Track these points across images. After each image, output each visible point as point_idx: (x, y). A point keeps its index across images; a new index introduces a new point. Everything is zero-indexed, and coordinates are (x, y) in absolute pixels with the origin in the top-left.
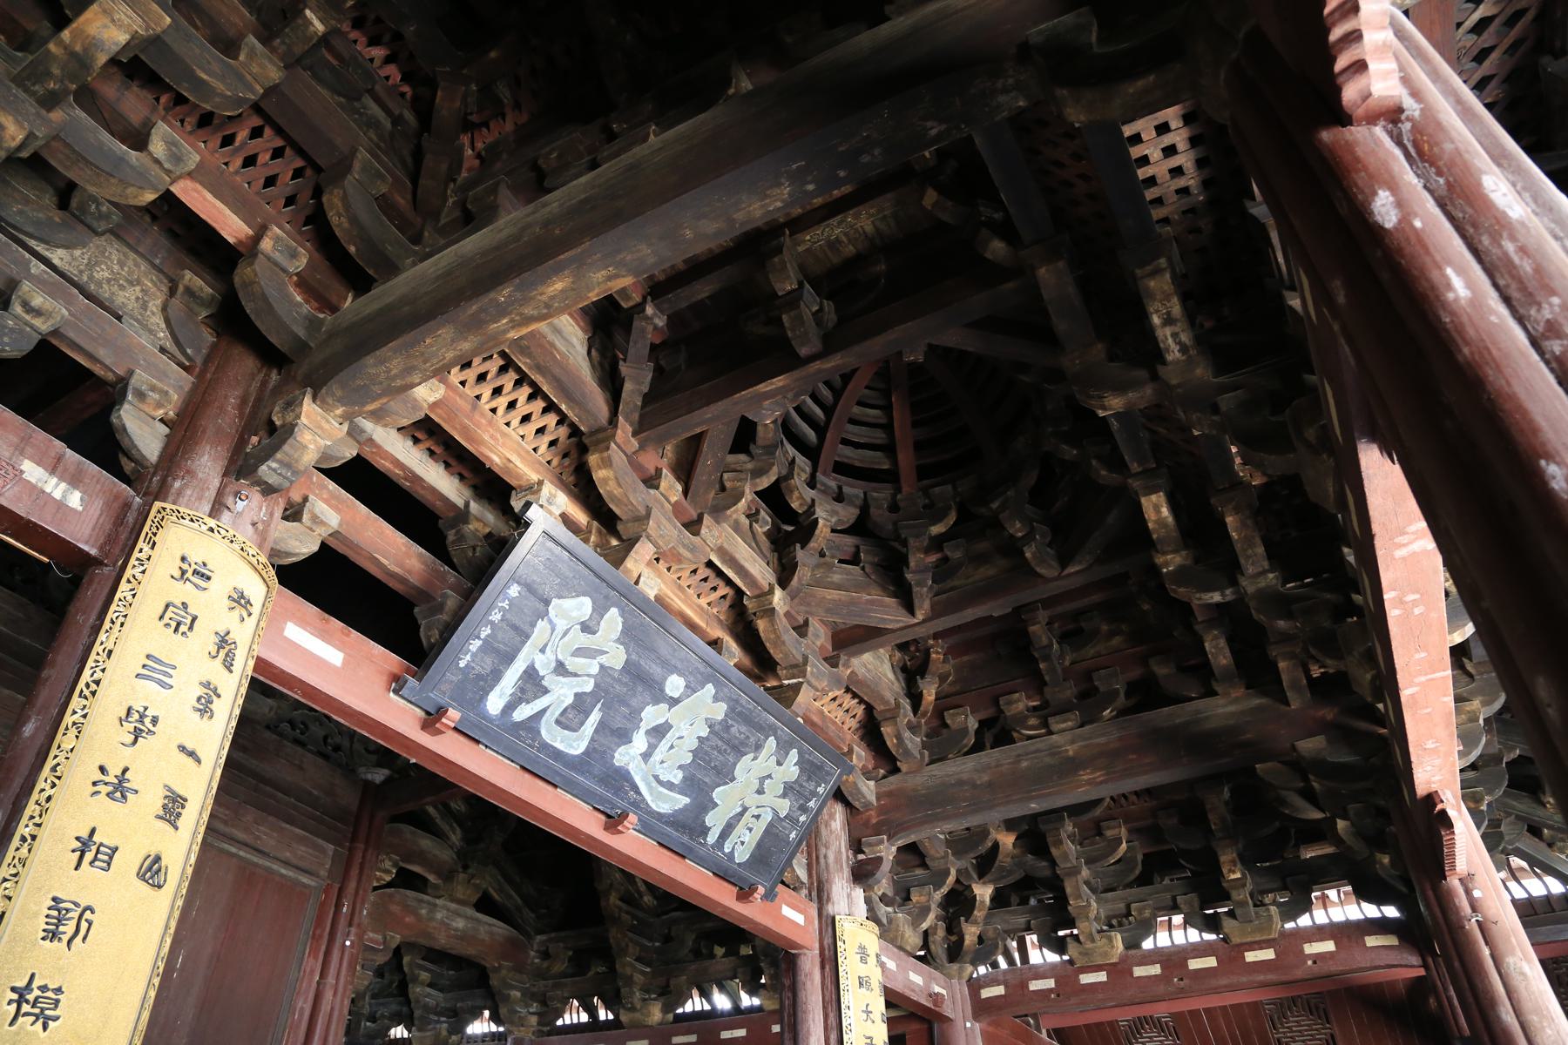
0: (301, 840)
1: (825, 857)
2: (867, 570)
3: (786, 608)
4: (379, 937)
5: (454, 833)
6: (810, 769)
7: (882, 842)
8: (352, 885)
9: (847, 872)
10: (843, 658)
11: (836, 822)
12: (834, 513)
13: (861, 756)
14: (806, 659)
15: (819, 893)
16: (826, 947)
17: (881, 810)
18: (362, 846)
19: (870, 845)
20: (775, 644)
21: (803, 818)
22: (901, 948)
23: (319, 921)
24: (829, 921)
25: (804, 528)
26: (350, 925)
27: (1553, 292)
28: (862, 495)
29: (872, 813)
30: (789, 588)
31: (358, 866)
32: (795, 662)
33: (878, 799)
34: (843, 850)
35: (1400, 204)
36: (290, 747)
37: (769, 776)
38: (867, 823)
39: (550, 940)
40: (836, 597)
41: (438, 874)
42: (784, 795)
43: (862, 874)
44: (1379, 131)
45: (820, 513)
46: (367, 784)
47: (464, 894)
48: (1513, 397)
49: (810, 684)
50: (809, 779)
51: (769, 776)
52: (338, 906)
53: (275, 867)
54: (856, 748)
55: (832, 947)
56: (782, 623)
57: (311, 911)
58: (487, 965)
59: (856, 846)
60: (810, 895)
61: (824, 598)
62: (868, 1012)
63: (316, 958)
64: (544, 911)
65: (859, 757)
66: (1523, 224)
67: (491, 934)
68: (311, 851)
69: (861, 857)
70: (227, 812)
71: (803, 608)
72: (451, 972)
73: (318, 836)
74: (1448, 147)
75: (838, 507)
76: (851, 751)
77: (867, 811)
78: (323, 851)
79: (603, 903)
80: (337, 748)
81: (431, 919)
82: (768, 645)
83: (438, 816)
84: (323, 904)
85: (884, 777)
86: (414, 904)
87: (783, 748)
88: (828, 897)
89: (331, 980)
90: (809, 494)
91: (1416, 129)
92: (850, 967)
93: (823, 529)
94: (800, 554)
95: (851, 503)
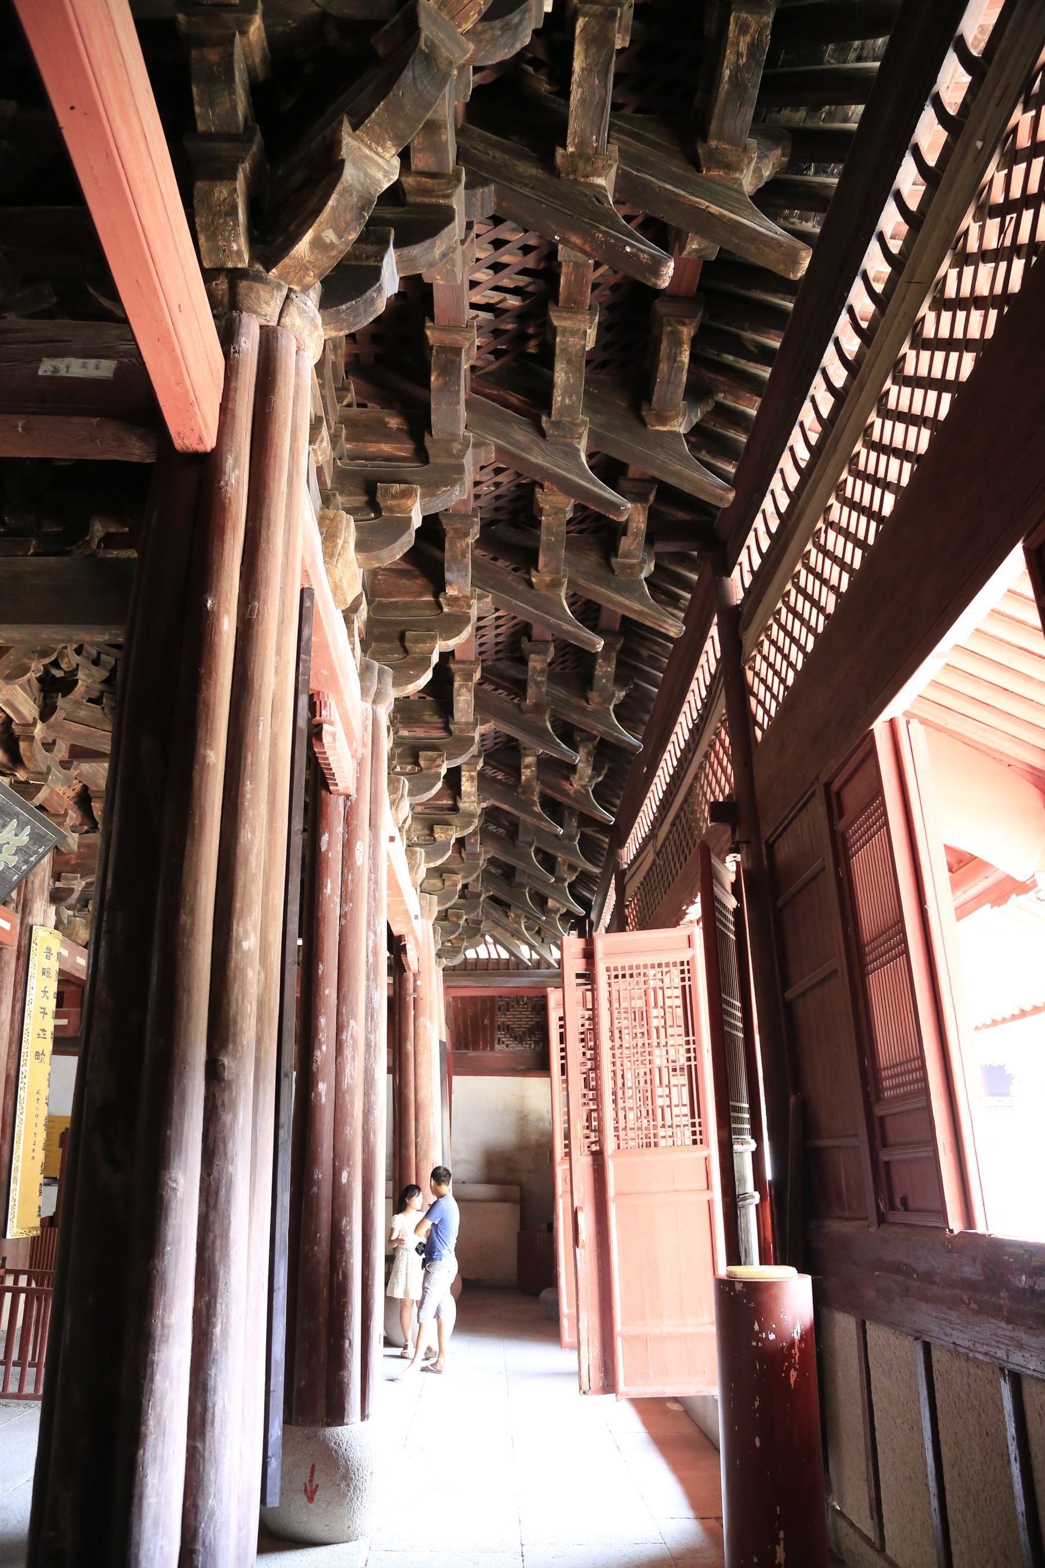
1: (33, 882)
2: (106, 710)
3: (42, 736)
6: (36, 838)
7: (76, 879)
9: (46, 894)
10: (75, 763)
11: (46, 861)
12: (91, 676)
13: (74, 816)
14: (49, 769)
15: (25, 908)
16: (23, 945)
17: (79, 855)
19: (67, 879)
20: (30, 759)
21: (24, 868)
22: (74, 941)
24: (28, 928)
25: (67, 684)
27: (352, 902)
28: (113, 662)
29: (73, 856)
30: (47, 723)
32: (39, 770)
33: (79, 847)
34: (47, 879)
35: (329, 843)
37: (8, 843)
38: (67, 863)
40: (79, 730)
42: (15, 854)
43: (56, 897)
44: (341, 799)
45: (81, 676)
48: (323, 938)
49: (48, 785)
50: (35, 844)
51: (8, 843)
54: (70, 812)
55: (27, 947)
56: (38, 744)
59: (57, 876)
60: (17, 908)
61: (71, 730)
62: (45, 992)
65: (71, 819)
66: (359, 868)
69: (58, 884)
71: (54, 734)
74: (355, 822)
75: (95, 670)
76: (66, 814)
77: (70, 854)
82: (24, 759)
85: (87, 832)
87: (21, 826)
88: (30, 911)
90: (75, 659)
91: (350, 807)
92: (37, 960)
93: (80, 688)
94: (61, 701)
95: (105, 668)
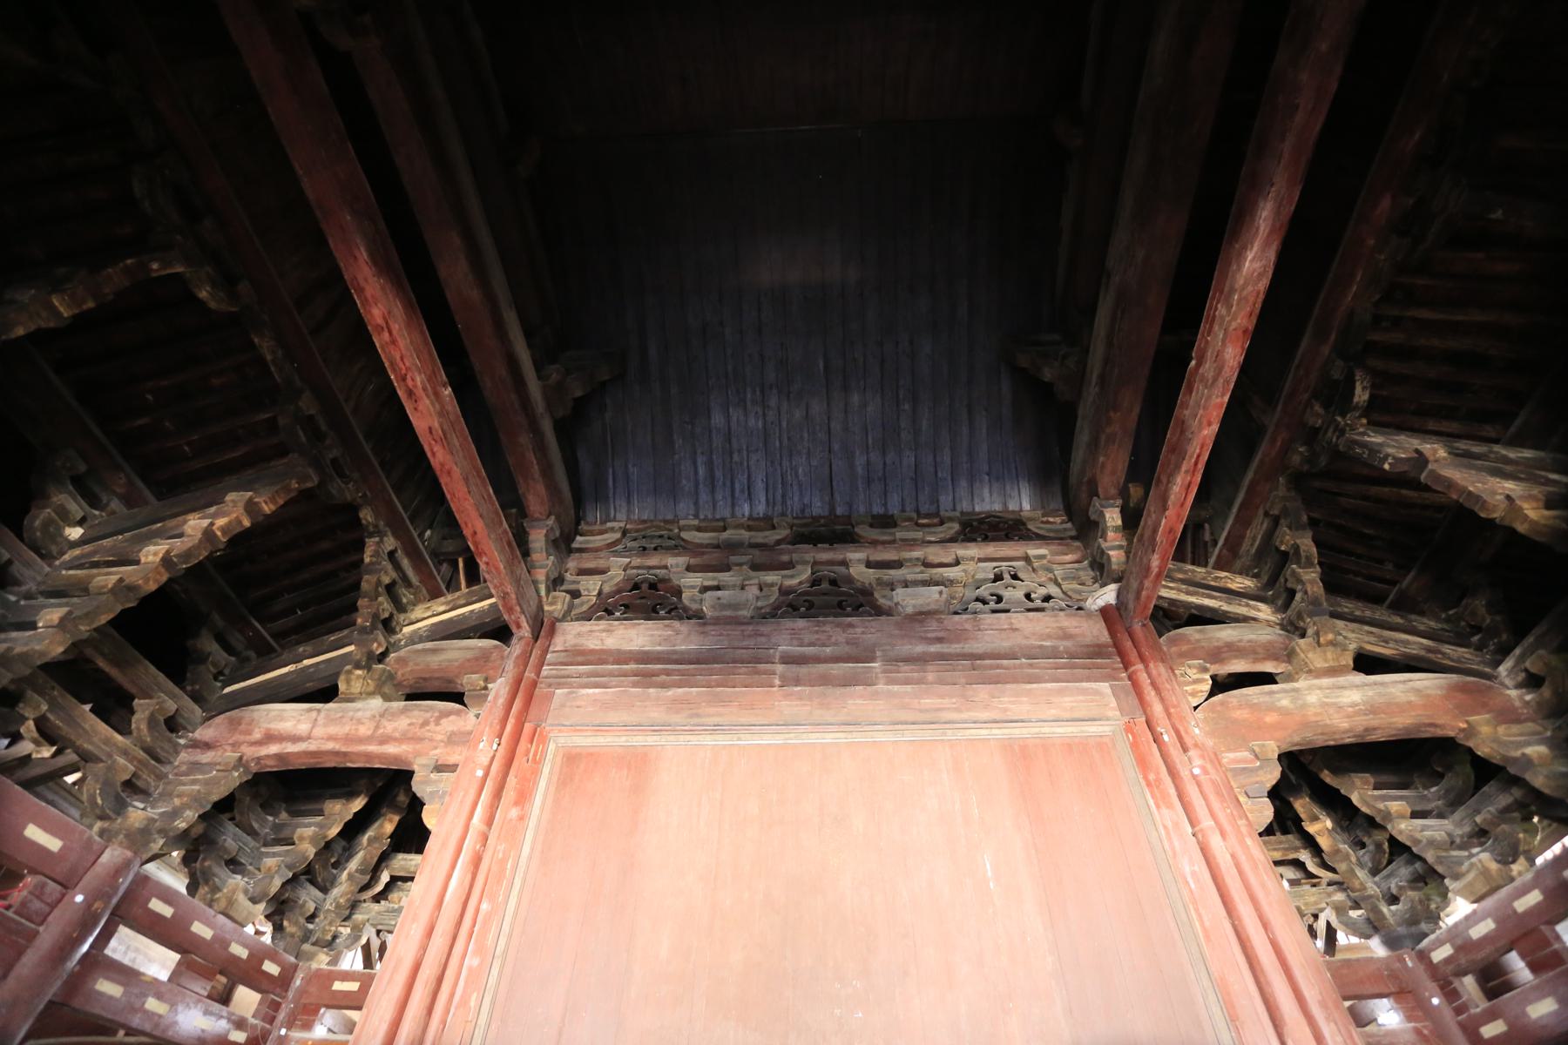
0: (1060, 692)
4: (1246, 754)
5: (1259, 610)
8: (1157, 708)
18: (1140, 666)
23: (1143, 763)
26: (1185, 750)
31: (1150, 688)
36: (989, 619)
39: (1521, 659)
41: (1275, 657)
46: (1105, 612)
47: (1326, 660)
52: (1157, 739)
53: (1046, 730)
57: (1128, 759)
58: (1451, 734)
63: (1170, 806)
64: (1475, 639)
67: (1417, 691)
68: (1081, 698)
70: (954, 700)
72: (1433, 789)
73: (1082, 681)
78: (1097, 692)
79: (1521, 528)
80: (1047, 598)
81: (1304, 706)
83: (1221, 603)
84: (1135, 746)
86: (1267, 699)
89: (1207, 823)
